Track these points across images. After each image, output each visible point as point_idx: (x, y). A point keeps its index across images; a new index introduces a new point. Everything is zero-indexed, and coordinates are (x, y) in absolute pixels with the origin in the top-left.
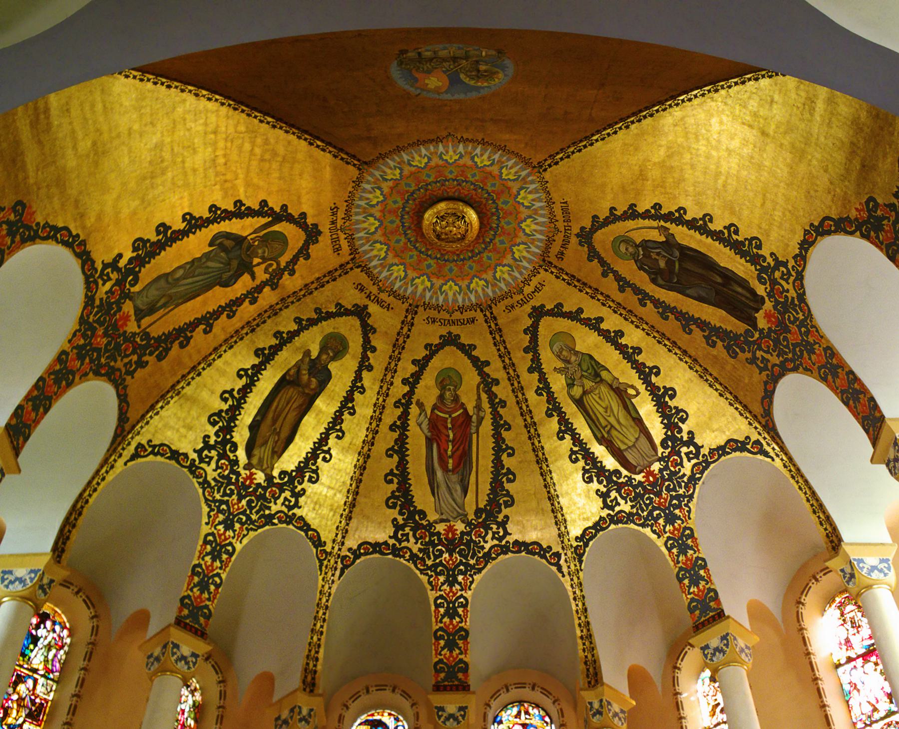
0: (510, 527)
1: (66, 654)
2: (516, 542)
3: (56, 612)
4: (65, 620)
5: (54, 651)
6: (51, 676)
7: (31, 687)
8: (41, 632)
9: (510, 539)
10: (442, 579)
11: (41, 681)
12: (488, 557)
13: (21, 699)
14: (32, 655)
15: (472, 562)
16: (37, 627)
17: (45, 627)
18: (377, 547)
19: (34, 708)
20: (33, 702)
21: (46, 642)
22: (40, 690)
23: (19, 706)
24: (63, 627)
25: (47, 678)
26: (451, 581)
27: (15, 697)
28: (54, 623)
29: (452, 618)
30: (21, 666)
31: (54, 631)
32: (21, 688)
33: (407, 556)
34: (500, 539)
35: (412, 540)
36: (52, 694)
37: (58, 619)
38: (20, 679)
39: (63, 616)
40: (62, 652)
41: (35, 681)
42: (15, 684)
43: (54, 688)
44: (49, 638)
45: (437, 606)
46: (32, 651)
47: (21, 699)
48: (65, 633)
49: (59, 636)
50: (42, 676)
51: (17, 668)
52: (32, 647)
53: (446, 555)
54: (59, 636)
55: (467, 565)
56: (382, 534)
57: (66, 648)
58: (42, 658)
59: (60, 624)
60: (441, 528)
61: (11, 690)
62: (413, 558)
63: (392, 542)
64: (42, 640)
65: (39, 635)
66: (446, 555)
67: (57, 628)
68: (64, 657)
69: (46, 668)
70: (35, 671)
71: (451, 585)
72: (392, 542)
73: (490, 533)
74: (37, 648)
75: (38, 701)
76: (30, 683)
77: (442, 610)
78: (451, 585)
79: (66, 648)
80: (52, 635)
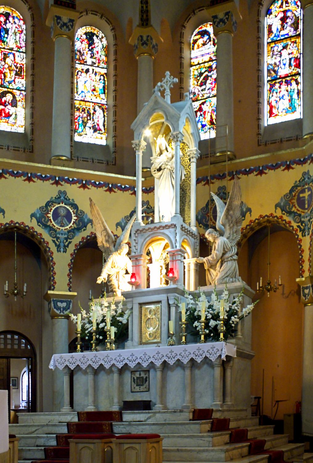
1: (26, 35)
3: (13, 10)
4: (20, 15)
5: (18, 35)
6: (21, 50)
7: (13, 60)
8: (9, 26)
11: (17, 54)
13: (10, 67)
14: (7, 40)
16: (6, 23)
17: (10, 22)
19: (18, 70)
20: (17, 68)
21: (13, 31)
22: (18, 60)
23: (10, 70)
24: (20, 20)
25: (20, 52)
27: (6, 66)
28: (13, 17)
30: (4, 48)
31: (15, 23)
32: (8, 60)
36: (25, 60)
37: (15, 15)
38: (5, 56)
39: (17, 12)
40: (23, 34)
41: (14, 55)
42: (4, 59)
43: (25, 57)
44: (14, 28)
46: (7, 38)
47: (10, 67)
48: (22, 22)
49: (19, 25)
50: (17, 51)
51: (3, 50)
52: (6, 36)
54: (19, 25)
57: (24, 32)
58: (14, 41)
59: (17, 17)
61: (3, 63)
64: (10, 30)
65: (8, 27)
67: (16, 20)
68: (25, 37)
69: (17, 46)
70: (12, 49)
74: (9, 36)
75: (18, 65)
76: (11, 56)
79: (24, 32)
80: (14, 26)
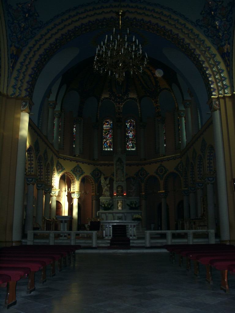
0: (129, 95)
2: (130, 98)
9: (129, 97)
10: (118, 104)
12: (125, 100)
15: (123, 101)
18: (107, 98)
26: (119, 104)
29: (119, 110)
33: (112, 100)
34: (127, 97)
35: (113, 97)
45: (117, 108)
53: (118, 100)
55: (122, 102)
56: (107, 96)
60: (117, 95)
62: (113, 100)
63: (109, 97)
66: (118, 100)
71: (119, 105)
72: (109, 97)
73: (126, 97)
77: (118, 109)
78: (119, 105)
